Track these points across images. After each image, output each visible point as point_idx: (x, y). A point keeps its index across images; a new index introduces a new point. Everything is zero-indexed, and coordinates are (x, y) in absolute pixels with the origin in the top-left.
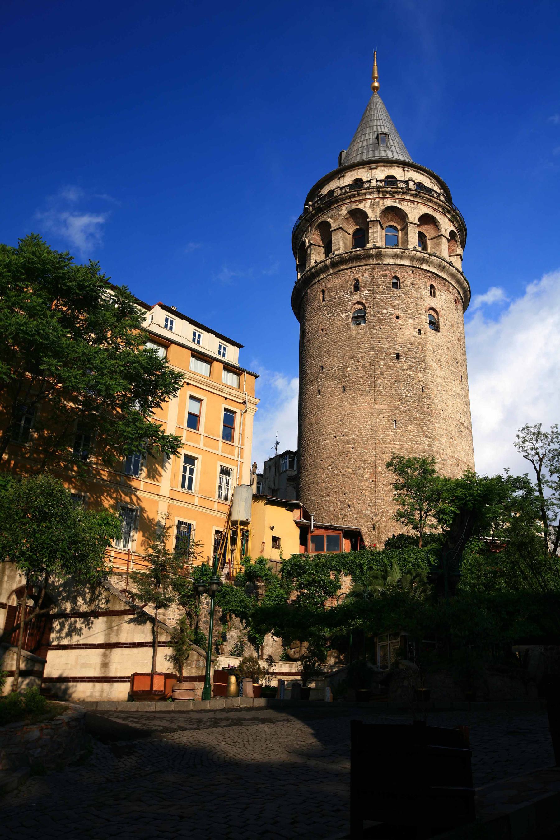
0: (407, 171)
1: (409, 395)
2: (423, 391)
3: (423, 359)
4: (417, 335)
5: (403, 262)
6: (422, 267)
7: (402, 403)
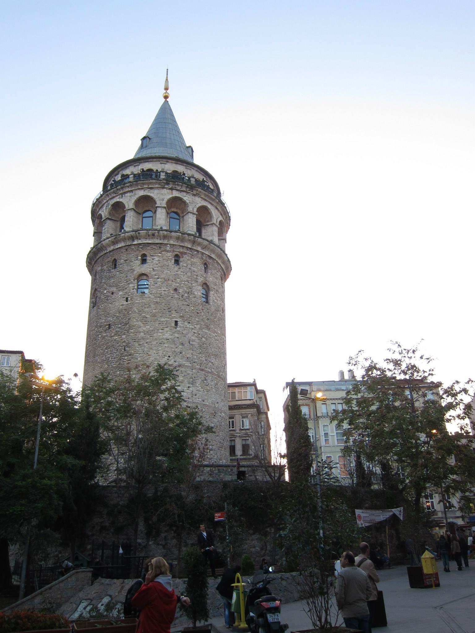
0: (137, 166)
1: (113, 357)
2: (125, 350)
3: (127, 322)
4: (125, 303)
5: (120, 245)
6: (134, 243)
7: (108, 366)
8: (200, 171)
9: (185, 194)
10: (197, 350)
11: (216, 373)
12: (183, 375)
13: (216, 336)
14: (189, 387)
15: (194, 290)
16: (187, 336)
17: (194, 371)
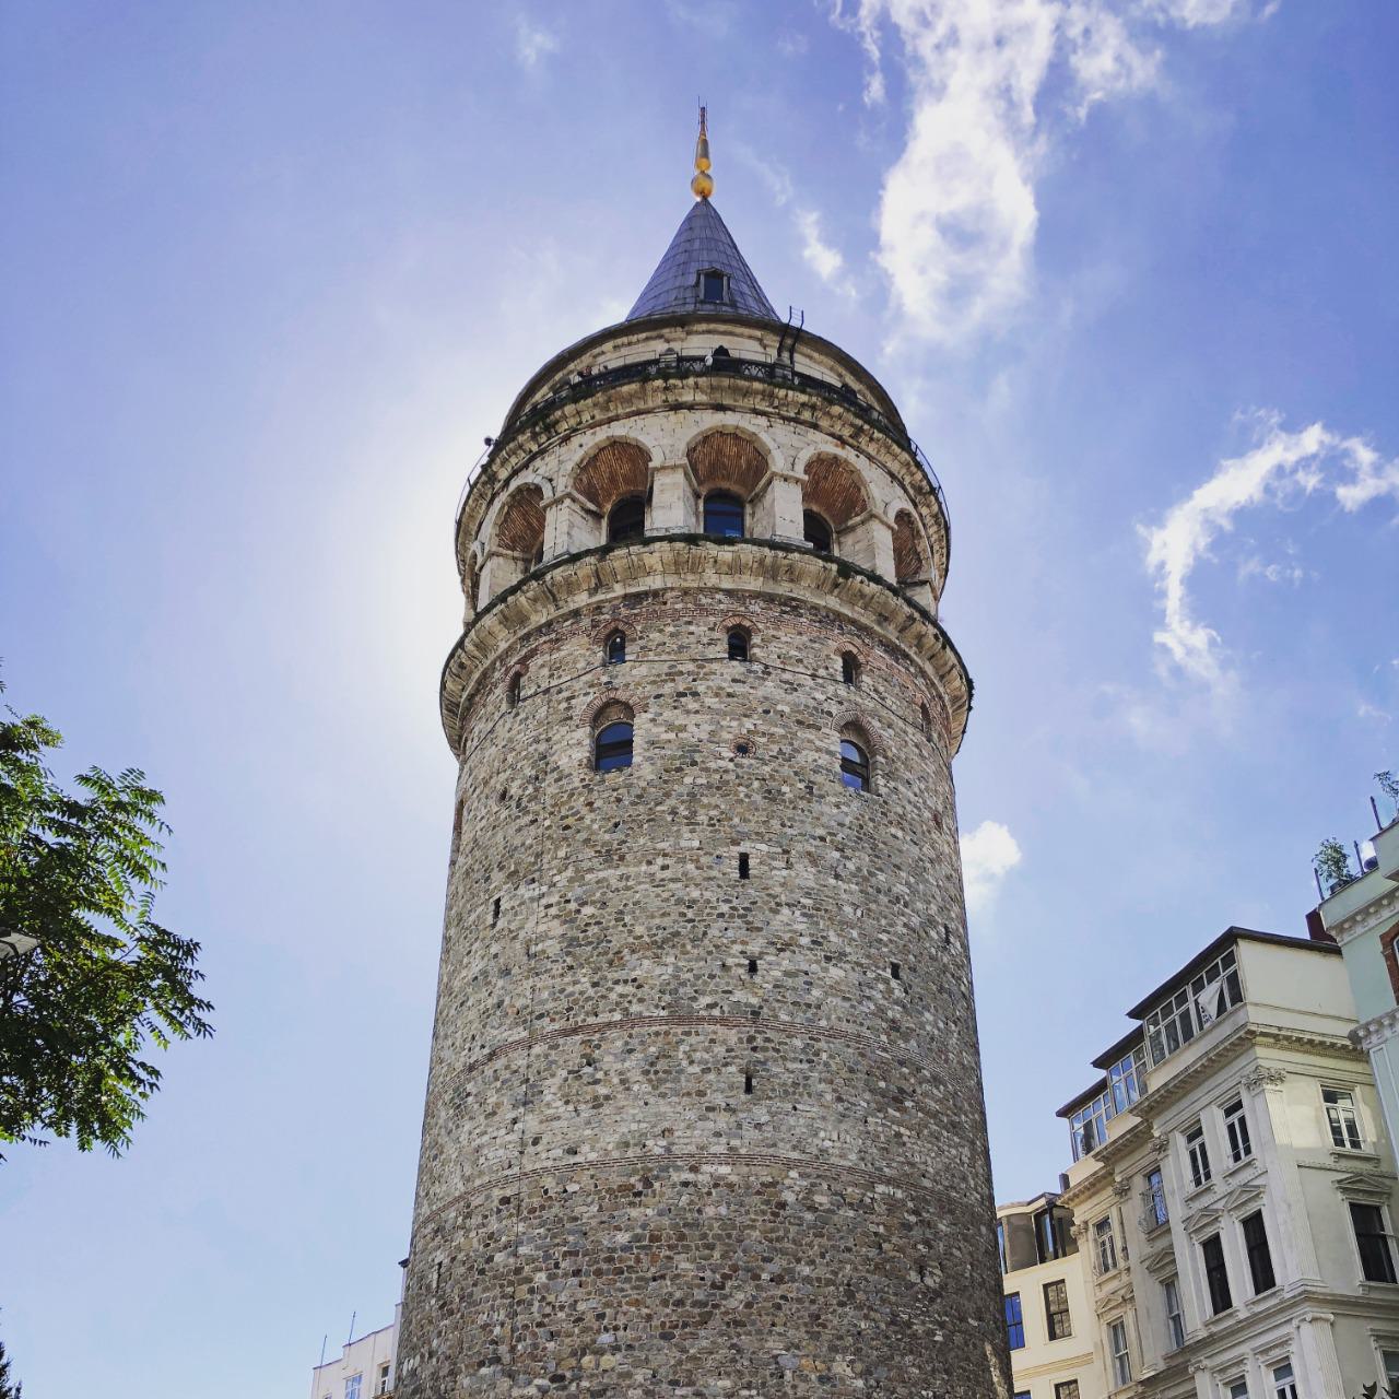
8: (625, 340)
9: (538, 463)
10: (555, 966)
11: (664, 1013)
12: (498, 1084)
13: (665, 868)
14: (515, 1121)
15: (555, 758)
16: (522, 934)
17: (537, 1050)
